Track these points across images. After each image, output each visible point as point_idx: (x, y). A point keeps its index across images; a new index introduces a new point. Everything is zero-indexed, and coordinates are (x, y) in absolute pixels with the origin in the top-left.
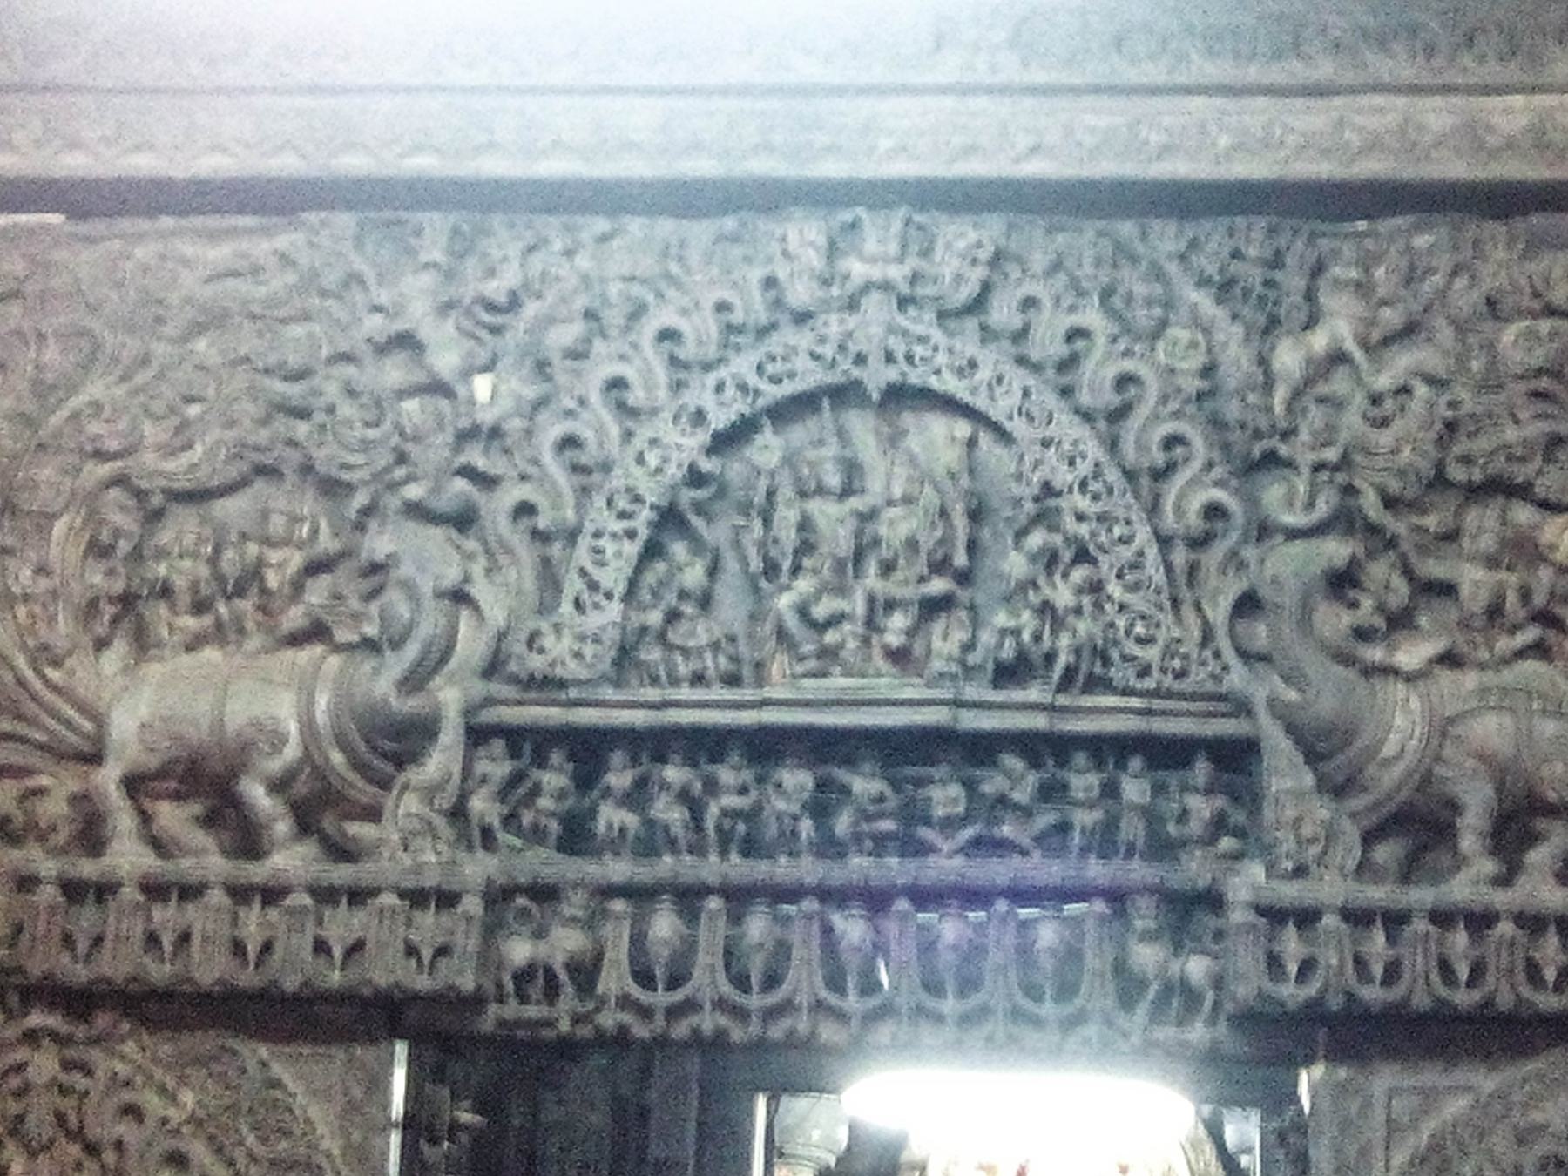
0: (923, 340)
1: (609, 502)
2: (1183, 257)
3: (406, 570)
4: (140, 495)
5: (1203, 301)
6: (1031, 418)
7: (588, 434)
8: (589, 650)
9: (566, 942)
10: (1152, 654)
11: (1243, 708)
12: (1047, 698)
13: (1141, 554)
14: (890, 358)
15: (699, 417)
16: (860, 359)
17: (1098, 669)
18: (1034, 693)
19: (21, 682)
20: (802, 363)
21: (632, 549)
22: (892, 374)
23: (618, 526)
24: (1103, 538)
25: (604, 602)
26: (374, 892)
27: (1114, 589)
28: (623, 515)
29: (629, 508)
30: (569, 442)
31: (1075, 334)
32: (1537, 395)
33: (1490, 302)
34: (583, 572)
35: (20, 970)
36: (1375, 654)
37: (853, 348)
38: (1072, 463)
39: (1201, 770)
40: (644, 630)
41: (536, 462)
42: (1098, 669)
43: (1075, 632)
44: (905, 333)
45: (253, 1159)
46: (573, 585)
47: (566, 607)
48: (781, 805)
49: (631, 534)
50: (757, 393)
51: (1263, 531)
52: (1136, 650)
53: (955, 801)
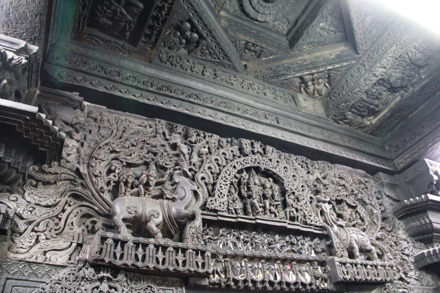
1: (222, 179)
3: (181, 185)
4: (122, 162)
5: (299, 167)
7: (213, 167)
8: (222, 204)
10: (312, 218)
12: (299, 223)
15: (235, 167)
16: (258, 163)
17: (304, 220)
18: (296, 223)
19: (93, 195)
20: (250, 162)
21: (227, 187)
22: (264, 166)
26: (187, 249)
27: (304, 207)
28: (224, 181)
30: (209, 168)
34: (219, 191)
35: (103, 260)
36: (338, 223)
37: (257, 161)
40: (231, 203)
43: (301, 213)
46: (217, 193)
47: (216, 196)
48: (256, 241)
49: (227, 185)
51: (319, 201)
52: (309, 217)
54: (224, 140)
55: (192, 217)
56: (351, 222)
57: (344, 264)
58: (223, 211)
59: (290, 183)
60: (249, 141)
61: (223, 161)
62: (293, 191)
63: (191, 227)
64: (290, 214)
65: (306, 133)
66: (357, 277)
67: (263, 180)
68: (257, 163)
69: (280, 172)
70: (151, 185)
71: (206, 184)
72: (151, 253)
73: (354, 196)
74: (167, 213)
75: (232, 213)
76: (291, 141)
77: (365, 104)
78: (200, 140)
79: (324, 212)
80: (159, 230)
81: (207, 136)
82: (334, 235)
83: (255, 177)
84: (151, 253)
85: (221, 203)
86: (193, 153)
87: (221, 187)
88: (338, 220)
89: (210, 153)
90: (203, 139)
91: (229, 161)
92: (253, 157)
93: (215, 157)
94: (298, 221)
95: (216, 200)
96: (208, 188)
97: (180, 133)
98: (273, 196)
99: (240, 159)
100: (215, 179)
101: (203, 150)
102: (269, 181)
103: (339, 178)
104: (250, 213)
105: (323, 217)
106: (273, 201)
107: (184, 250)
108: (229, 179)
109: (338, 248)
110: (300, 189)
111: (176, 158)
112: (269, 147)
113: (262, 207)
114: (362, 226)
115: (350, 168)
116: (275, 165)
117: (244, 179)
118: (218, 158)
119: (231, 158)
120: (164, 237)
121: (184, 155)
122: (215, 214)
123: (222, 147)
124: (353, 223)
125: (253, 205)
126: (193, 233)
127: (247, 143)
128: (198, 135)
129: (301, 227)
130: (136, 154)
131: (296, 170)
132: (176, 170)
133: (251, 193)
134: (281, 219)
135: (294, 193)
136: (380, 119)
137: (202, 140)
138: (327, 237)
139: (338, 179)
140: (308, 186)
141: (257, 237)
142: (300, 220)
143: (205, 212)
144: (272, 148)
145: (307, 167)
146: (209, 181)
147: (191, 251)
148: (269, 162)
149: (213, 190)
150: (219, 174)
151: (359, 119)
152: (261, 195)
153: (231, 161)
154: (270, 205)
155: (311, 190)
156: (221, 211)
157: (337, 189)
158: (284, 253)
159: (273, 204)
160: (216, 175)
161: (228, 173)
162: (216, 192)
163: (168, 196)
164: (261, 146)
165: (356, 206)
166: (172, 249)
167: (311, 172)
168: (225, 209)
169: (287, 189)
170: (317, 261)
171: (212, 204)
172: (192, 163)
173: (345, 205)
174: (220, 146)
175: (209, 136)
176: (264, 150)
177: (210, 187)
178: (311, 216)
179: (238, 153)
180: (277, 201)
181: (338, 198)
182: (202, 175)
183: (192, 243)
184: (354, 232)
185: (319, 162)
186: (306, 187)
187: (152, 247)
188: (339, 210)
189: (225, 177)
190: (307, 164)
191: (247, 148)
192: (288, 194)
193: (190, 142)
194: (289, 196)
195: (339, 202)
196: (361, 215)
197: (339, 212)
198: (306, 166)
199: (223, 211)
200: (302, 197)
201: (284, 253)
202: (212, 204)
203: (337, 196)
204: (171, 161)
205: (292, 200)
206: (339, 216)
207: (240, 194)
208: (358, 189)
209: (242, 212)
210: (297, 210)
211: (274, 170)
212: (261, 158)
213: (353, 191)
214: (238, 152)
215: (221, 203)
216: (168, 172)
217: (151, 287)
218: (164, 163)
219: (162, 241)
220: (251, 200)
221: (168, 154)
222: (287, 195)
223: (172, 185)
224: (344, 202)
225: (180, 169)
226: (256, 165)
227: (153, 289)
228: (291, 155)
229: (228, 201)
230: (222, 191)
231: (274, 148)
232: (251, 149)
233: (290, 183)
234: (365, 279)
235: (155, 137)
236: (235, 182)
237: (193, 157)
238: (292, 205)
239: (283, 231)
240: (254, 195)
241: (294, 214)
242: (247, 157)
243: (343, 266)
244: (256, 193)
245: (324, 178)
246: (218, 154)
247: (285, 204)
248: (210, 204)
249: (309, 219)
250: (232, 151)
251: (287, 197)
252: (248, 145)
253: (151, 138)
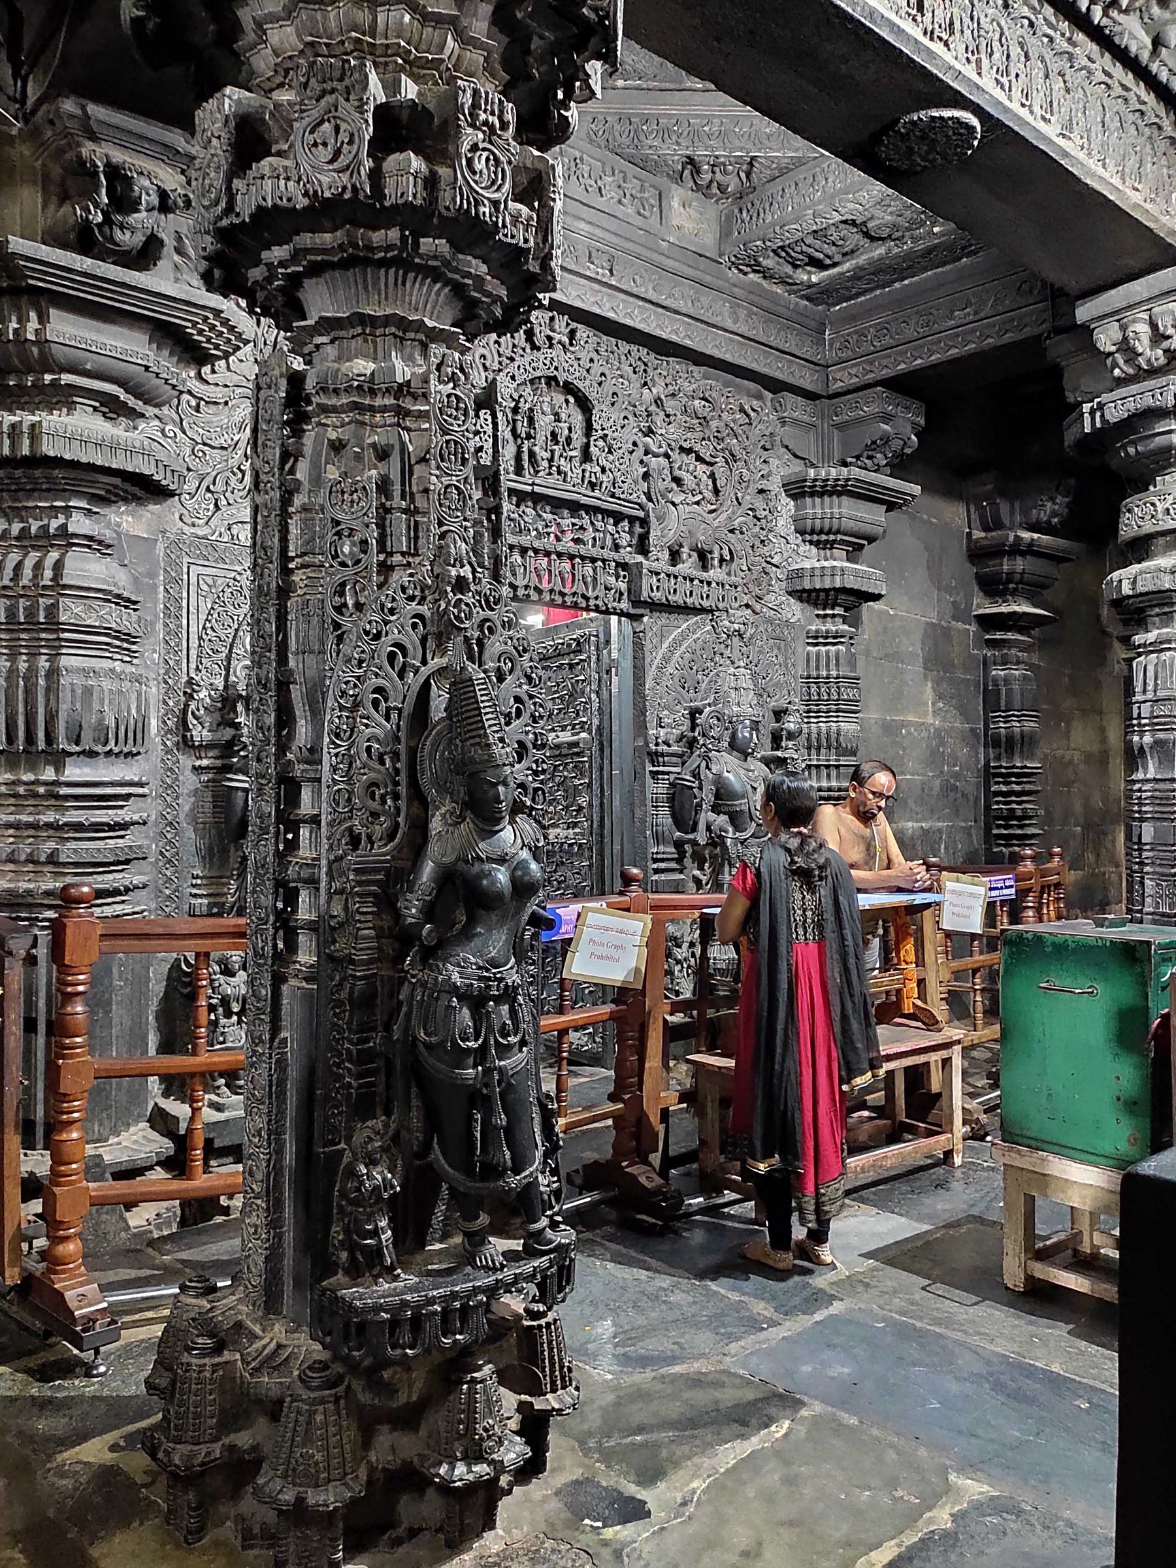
11: (642, 507)
15: (513, 378)
18: (597, 493)
31: (603, 374)
39: (625, 524)
57: (657, 574)
65: (661, 299)
77: (805, 248)
93: (482, 351)
98: (569, 440)
102: (567, 401)
118: (486, 352)
136: (830, 277)
138: (644, 522)
151: (789, 269)
169: (595, 426)
176: (572, 333)
210: (603, 470)
211: (580, 385)
226: (551, 372)
239: (575, 507)
247: (586, 457)
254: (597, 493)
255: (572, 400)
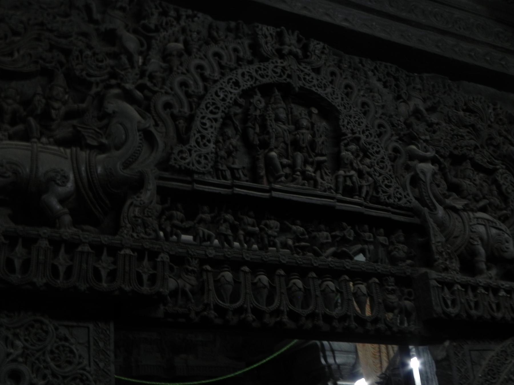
0: (309, 75)
1: (207, 108)
2: (373, 71)
5: (379, 85)
6: (345, 109)
8: (203, 161)
9: (188, 282)
10: (391, 191)
13: (383, 158)
14: (299, 79)
15: (237, 84)
16: (289, 76)
17: (375, 194)
18: (356, 199)
20: (270, 73)
21: (217, 125)
22: (301, 83)
23: (211, 116)
24: (371, 151)
25: (207, 143)
26: (120, 249)
27: (377, 168)
28: (212, 112)
29: (214, 110)
32: (468, 132)
33: (456, 103)
34: (199, 132)
36: (448, 201)
37: (287, 72)
38: (359, 125)
39: (400, 235)
40: (222, 157)
41: (172, 89)
42: (375, 194)
44: (302, 71)
45: (54, 375)
46: (194, 136)
47: (193, 143)
48: (270, 232)
49: (216, 120)
50: (256, 79)
53: (327, 238)
54: (222, 25)
55: (138, 184)
56: (477, 201)
57: (450, 285)
58: (204, 174)
59: (352, 120)
60: (272, 30)
61: (213, 71)
62: (357, 135)
63: (132, 204)
64: (345, 181)
66: (473, 312)
67: (299, 110)
68: (285, 77)
69: (335, 96)
70: (54, 116)
71: (174, 117)
72: (41, 257)
73: (492, 148)
74: (84, 174)
75: (225, 178)
76: (365, 30)
78: (167, 24)
79: (420, 179)
80: (66, 210)
81: (184, 17)
82: (435, 225)
83: (279, 105)
84: (41, 257)
85: (200, 156)
86: (150, 53)
87: (204, 124)
88: (447, 197)
89: (189, 52)
90: (175, 23)
91: (228, 70)
92: (279, 64)
94: (360, 196)
95: (190, 151)
96: (177, 127)
97: (122, 9)
98: (312, 144)
99: (251, 67)
100: (194, 106)
101: (173, 45)
103: (464, 110)
104: (262, 177)
105: (417, 190)
106: (312, 154)
107: (113, 251)
108: (222, 109)
109: (441, 253)
110: (372, 131)
111: (110, 62)
112: (316, 42)
113: (289, 166)
114: (501, 210)
115: (492, 90)
116: (324, 81)
117: (256, 109)
119: (233, 64)
120: (76, 223)
121: (130, 58)
122: (189, 179)
123: (216, 42)
124: (482, 204)
125: (269, 162)
126: (135, 217)
127: (267, 33)
128: (164, 13)
129: (366, 207)
130: (22, 52)
131: (371, 91)
132: (111, 87)
133: (266, 137)
134: (325, 191)
135: (358, 139)
137: (172, 25)
138: (422, 230)
139: (461, 113)
140: (393, 125)
141: (272, 225)
142: (363, 195)
143: (167, 175)
144: (322, 44)
145: (397, 86)
146: (180, 111)
147: (128, 252)
148: (313, 74)
149: (189, 129)
150: (201, 98)
152: (289, 142)
153: (231, 70)
154: (306, 162)
155: (398, 134)
156: (198, 173)
157: (455, 132)
158: (327, 257)
159: (311, 160)
160: (195, 100)
161: (222, 95)
162: (192, 134)
163: (90, 141)
164: (299, 41)
165: (495, 170)
166: (87, 248)
167: (404, 96)
168: (209, 168)
169: (344, 130)
170: (392, 275)
171: (182, 158)
172: (147, 73)
173: (469, 166)
174: (211, 39)
175: (188, 17)
176: (305, 48)
177: (182, 123)
178: (388, 186)
179: (248, 54)
180: (322, 155)
181: (456, 152)
182: (165, 98)
183: (132, 236)
184: (480, 221)
185: (425, 75)
186: (388, 128)
187: (44, 243)
188: (456, 176)
189: (214, 104)
190: (396, 79)
191: (266, 43)
192: (346, 141)
193: (146, 28)
194: (346, 145)
195: (457, 160)
196: (504, 187)
197: (455, 180)
198: (394, 83)
199: (204, 174)
200: (375, 149)
201: (327, 257)
202: (182, 158)
203: (456, 148)
204: (100, 68)
205: (353, 153)
206: (455, 188)
207: (245, 138)
208: (504, 133)
209: (245, 175)
211: (320, 91)
212: (295, 66)
213: (491, 138)
214: (249, 53)
215: (200, 156)
216: (94, 90)
217: (42, 323)
218: (84, 73)
219: (68, 231)
220: (267, 151)
221: (94, 54)
222: (342, 143)
223: (100, 119)
224: (468, 161)
225: (119, 86)
227: (44, 327)
228: (364, 59)
229: (216, 153)
230: (204, 132)
231: (326, 46)
232: (277, 46)
233: (352, 120)
234: (489, 317)
235: (67, 15)
236: (236, 114)
237: (150, 59)
238: (351, 164)
239: (329, 217)
240: (273, 142)
241: (353, 183)
242: (266, 64)
243: (446, 289)
244: (277, 138)
245: (432, 110)
246: (205, 56)
247: (338, 162)
248: (178, 158)
249: (384, 192)
250: (235, 50)
251: (343, 147)
252: (269, 38)
253: (58, 18)
254: (356, 199)
255: (315, 111)
